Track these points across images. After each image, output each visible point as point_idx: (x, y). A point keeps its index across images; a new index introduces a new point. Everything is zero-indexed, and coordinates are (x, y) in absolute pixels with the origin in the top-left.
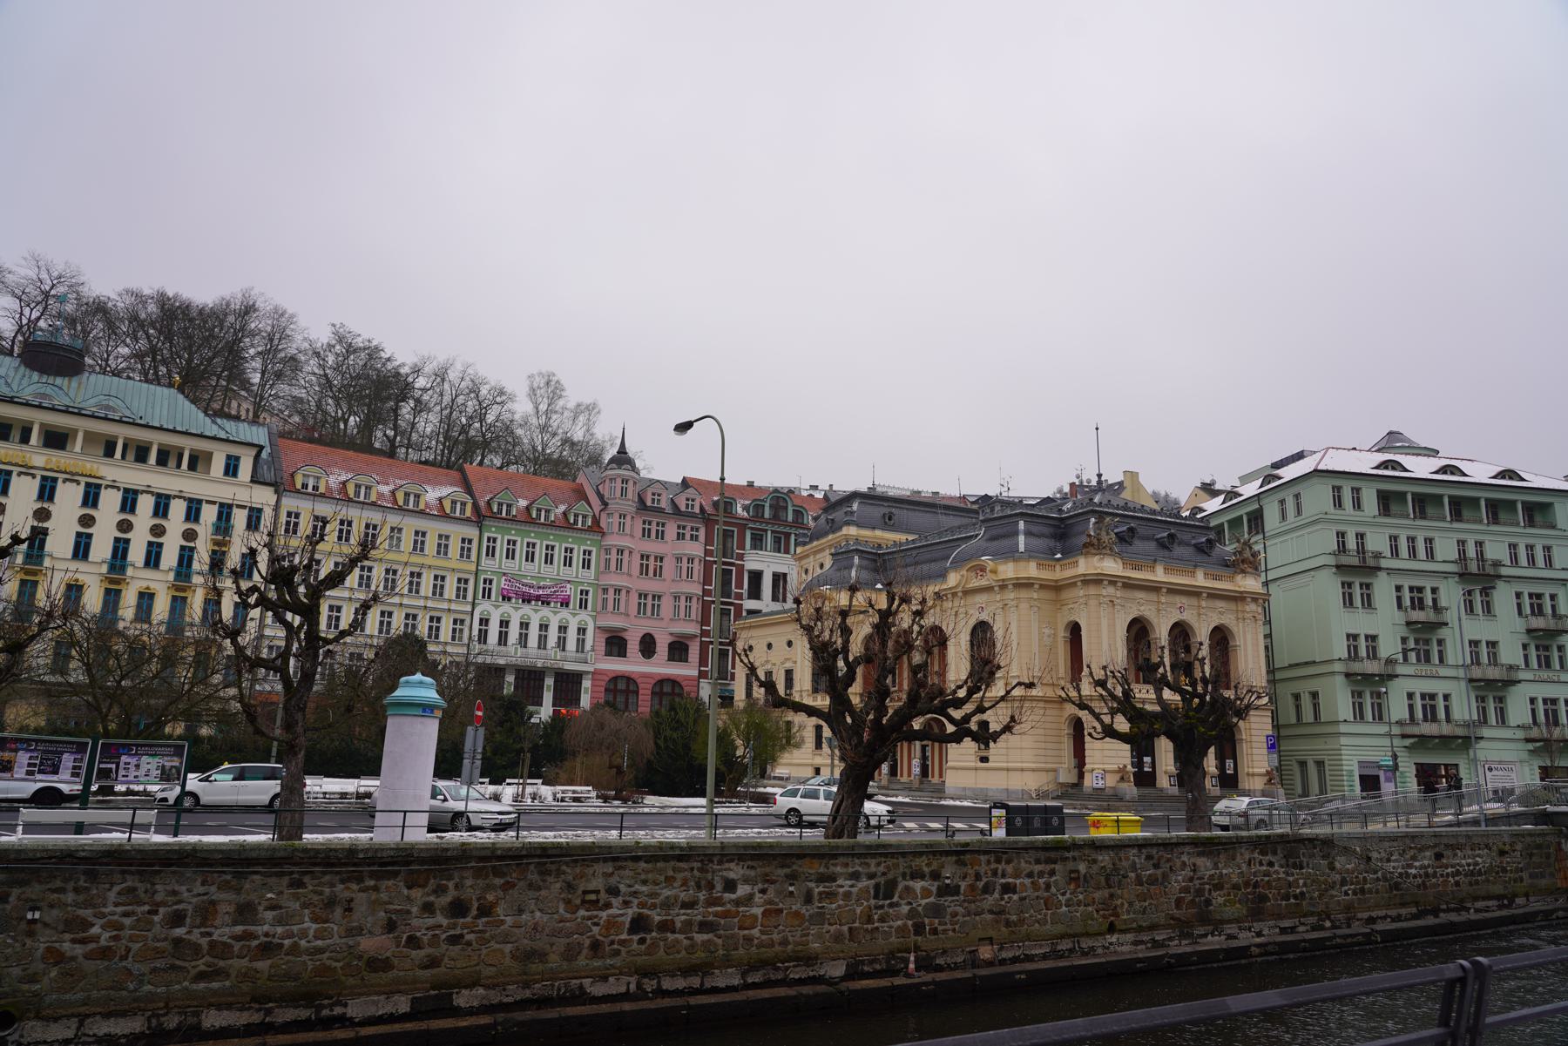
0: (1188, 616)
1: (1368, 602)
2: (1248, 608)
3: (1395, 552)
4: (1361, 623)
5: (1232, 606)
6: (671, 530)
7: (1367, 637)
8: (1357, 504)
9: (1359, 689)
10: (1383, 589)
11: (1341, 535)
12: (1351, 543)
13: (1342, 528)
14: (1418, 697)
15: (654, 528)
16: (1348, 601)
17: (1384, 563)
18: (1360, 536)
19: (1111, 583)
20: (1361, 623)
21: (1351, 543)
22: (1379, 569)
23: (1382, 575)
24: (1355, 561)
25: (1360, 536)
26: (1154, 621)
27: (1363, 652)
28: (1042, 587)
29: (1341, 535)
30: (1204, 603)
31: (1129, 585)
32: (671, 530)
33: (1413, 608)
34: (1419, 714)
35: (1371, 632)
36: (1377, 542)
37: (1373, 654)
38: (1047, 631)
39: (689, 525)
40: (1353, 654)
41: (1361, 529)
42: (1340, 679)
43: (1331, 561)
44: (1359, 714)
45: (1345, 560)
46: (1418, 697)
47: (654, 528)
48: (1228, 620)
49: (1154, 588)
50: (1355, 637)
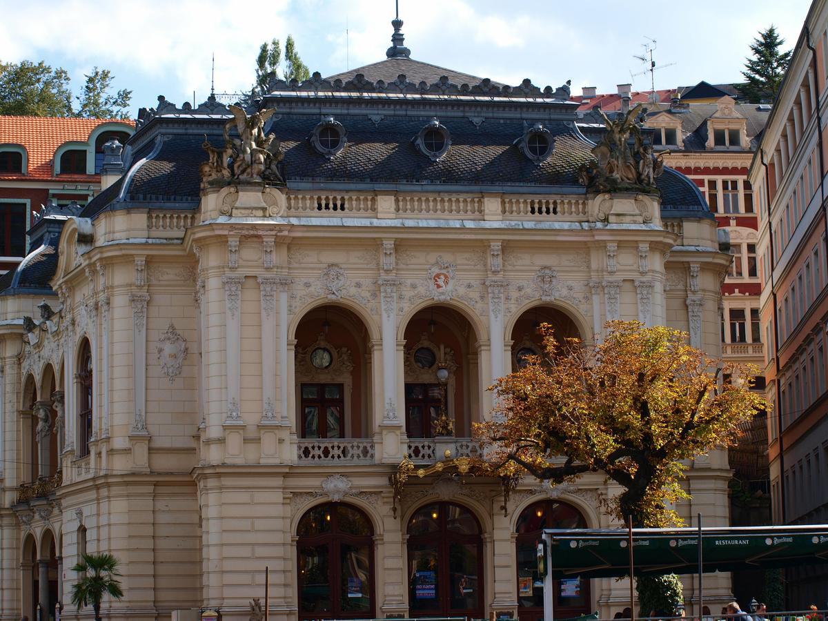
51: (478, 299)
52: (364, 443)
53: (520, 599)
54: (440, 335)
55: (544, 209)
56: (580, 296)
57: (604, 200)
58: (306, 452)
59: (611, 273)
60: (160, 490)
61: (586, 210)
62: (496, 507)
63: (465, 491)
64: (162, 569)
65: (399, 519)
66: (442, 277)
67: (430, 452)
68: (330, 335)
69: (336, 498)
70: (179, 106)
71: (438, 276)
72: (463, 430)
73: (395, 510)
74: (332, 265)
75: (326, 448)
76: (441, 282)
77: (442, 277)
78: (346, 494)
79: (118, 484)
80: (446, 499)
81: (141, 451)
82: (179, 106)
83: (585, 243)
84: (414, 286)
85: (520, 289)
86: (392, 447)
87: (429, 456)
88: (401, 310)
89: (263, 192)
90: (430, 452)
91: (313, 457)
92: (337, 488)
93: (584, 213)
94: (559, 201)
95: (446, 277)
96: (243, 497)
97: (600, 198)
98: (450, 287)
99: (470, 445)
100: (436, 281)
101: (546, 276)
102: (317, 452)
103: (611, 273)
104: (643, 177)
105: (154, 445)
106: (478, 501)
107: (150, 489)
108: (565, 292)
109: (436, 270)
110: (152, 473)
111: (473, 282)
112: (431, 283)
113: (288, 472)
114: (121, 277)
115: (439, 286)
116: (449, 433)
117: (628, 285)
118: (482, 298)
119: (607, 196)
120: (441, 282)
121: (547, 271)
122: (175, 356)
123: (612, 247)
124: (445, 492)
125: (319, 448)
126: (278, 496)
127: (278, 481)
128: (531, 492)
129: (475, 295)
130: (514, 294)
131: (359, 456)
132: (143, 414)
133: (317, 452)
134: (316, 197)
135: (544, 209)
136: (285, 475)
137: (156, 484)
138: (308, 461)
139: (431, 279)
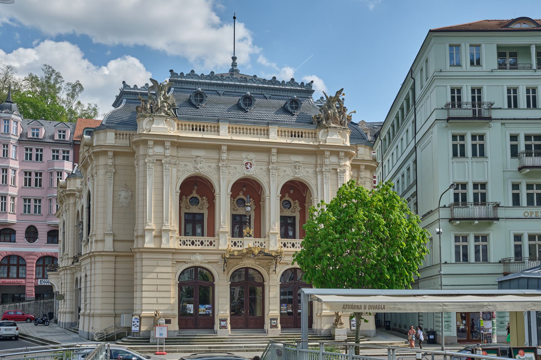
0: (256, 172)
1: (480, 151)
2: (327, 161)
3: (513, 103)
4: (470, 171)
5: (311, 160)
6: (48, 154)
7: (475, 186)
8: (476, 62)
9: (464, 233)
10: (496, 138)
11: (456, 92)
12: (467, 97)
13: (456, 84)
14: (525, 239)
15: (34, 153)
16: (458, 152)
17: (495, 114)
18: (477, 92)
19: (156, 143)
20: (470, 171)
21: (467, 97)
22: (490, 119)
23: (496, 126)
24: (470, 114)
25: (477, 92)
26: (213, 177)
27: (470, 199)
28: (116, 154)
29: (456, 92)
30: (274, 159)
31: (179, 144)
32: (48, 154)
33: (529, 154)
34: (526, 253)
35: (480, 179)
36: (494, 95)
37: (481, 199)
38: (123, 194)
39: (61, 149)
40: (460, 200)
41: (477, 84)
42: (443, 227)
43: (444, 115)
44: (462, 256)
45: (455, 113)
46: (525, 239)
47: (34, 153)
48: (305, 173)
49: (215, 147)
50: (464, 186)
52: (211, 239)
53: (281, 314)
54: (248, 190)
55: (297, 135)
60: (118, 259)
62: (271, 270)
63: (257, 263)
64: (118, 295)
65: (226, 275)
67: (241, 244)
68: (196, 189)
69: (197, 264)
70: (132, 87)
71: (247, 163)
72: (258, 234)
74: (198, 156)
75: (193, 241)
76: (248, 166)
78: (202, 263)
79: (98, 255)
80: (248, 266)
81: (109, 241)
82: (132, 87)
85: (285, 171)
86: (225, 242)
87: (241, 246)
90: (241, 244)
92: (198, 260)
93: (315, 138)
95: (251, 164)
96: (154, 263)
99: (260, 242)
104: (342, 122)
105: (116, 238)
107: (113, 259)
108: (305, 174)
109: (245, 161)
110: (114, 251)
111: (263, 167)
112: (244, 166)
113: (174, 252)
114: (102, 161)
115: (247, 168)
116: (250, 236)
117: (334, 171)
121: (297, 163)
122: (126, 198)
123: (328, 153)
124: (248, 263)
125: (190, 241)
126: (170, 263)
127: (170, 256)
131: (208, 245)
132: (111, 224)
133: (189, 243)
135: (297, 135)
136: (173, 253)
137: (116, 256)
138: (185, 247)
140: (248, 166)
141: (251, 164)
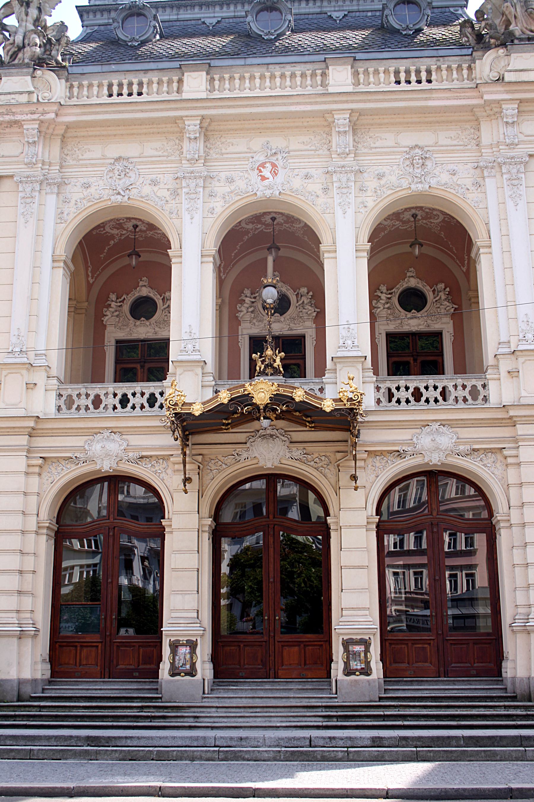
51: (320, 192)
56: (468, 183)
57: (498, 57)
58: (69, 403)
59: (512, 145)
61: (473, 76)
62: (345, 478)
63: (297, 454)
66: (268, 165)
71: (263, 165)
73: (187, 480)
77: (268, 165)
83: (471, 109)
84: (230, 180)
85: (380, 176)
88: (212, 211)
89: (33, 77)
91: (78, 408)
94: (434, 67)
95: (274, 165)
97: (491, 55)
98: (280, 179)
100: (260, 171)
101: (418, 158)
102: (83, 402)
103: (512, 145)
106: (317, 469)
109: (261, 158)
111: (312, 172)
112: (254, 176)
113: (36, 428)
115: (263, 178)
116: (276, 372)
118: (326, 190)
119: (501, 51)
120: (266, 173)
128: (399, 454)
129: (315, 187)
130: (372, 184)
133: (83, 402)
134: (105, 83)
139: (253, 170)
140: (266, 173)
141: (274, 165)
